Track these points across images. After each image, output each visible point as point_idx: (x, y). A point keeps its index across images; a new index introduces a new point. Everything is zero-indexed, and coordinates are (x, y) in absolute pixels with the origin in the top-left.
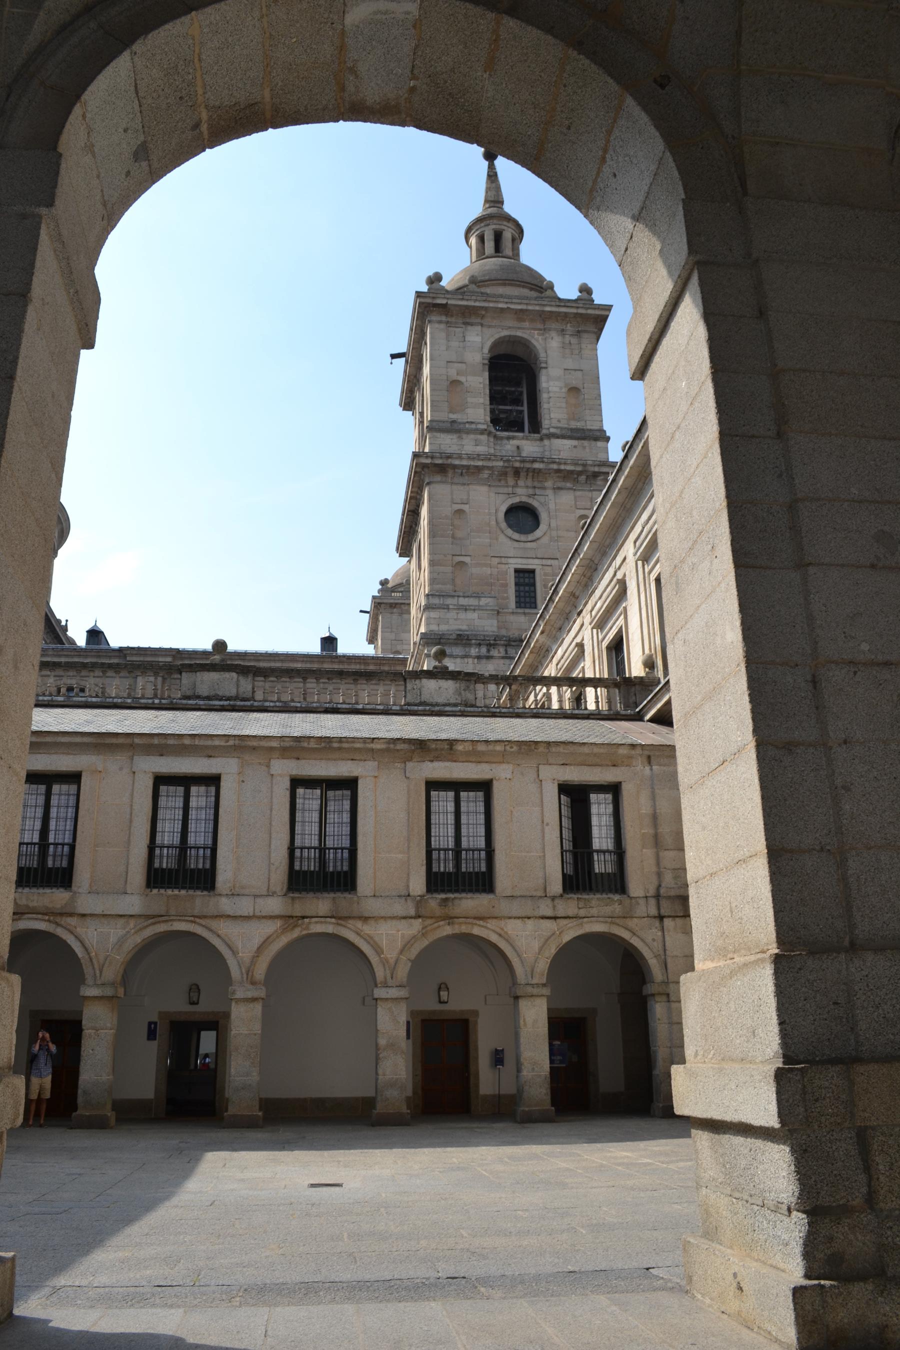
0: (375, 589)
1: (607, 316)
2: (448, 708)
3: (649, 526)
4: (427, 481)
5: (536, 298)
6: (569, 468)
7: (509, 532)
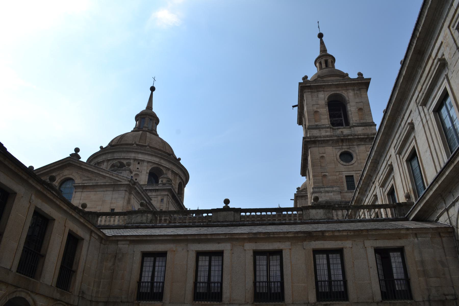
0: (295, 191)
2: (321, 221)
3: (400, 139)
4: (309, 146)
5: (343, 80)
6: (362, 137)
7: (342, 162)
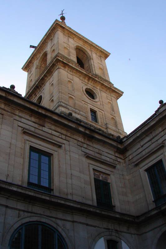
1: (109, 56)
